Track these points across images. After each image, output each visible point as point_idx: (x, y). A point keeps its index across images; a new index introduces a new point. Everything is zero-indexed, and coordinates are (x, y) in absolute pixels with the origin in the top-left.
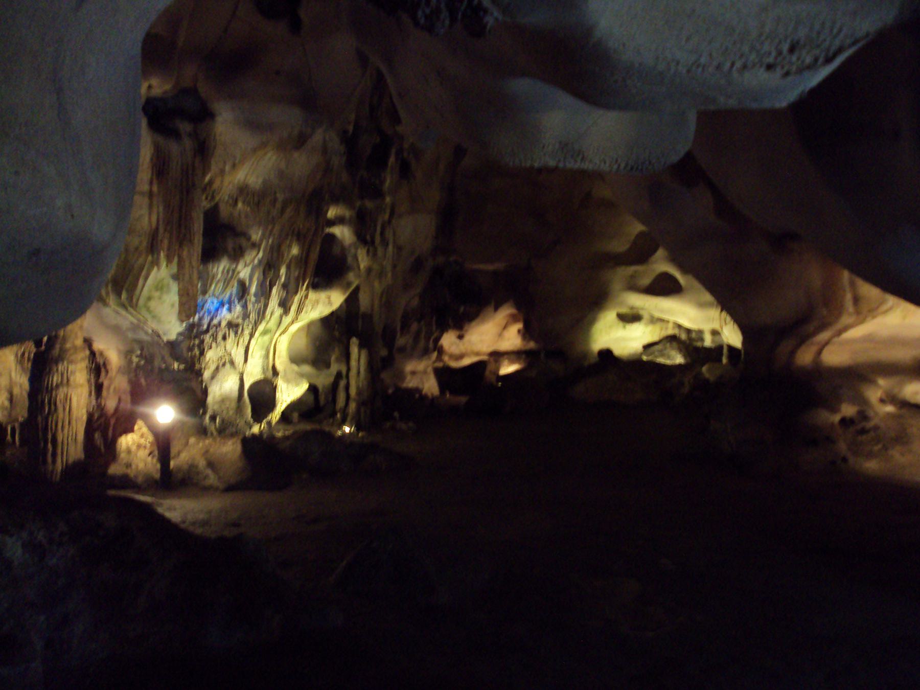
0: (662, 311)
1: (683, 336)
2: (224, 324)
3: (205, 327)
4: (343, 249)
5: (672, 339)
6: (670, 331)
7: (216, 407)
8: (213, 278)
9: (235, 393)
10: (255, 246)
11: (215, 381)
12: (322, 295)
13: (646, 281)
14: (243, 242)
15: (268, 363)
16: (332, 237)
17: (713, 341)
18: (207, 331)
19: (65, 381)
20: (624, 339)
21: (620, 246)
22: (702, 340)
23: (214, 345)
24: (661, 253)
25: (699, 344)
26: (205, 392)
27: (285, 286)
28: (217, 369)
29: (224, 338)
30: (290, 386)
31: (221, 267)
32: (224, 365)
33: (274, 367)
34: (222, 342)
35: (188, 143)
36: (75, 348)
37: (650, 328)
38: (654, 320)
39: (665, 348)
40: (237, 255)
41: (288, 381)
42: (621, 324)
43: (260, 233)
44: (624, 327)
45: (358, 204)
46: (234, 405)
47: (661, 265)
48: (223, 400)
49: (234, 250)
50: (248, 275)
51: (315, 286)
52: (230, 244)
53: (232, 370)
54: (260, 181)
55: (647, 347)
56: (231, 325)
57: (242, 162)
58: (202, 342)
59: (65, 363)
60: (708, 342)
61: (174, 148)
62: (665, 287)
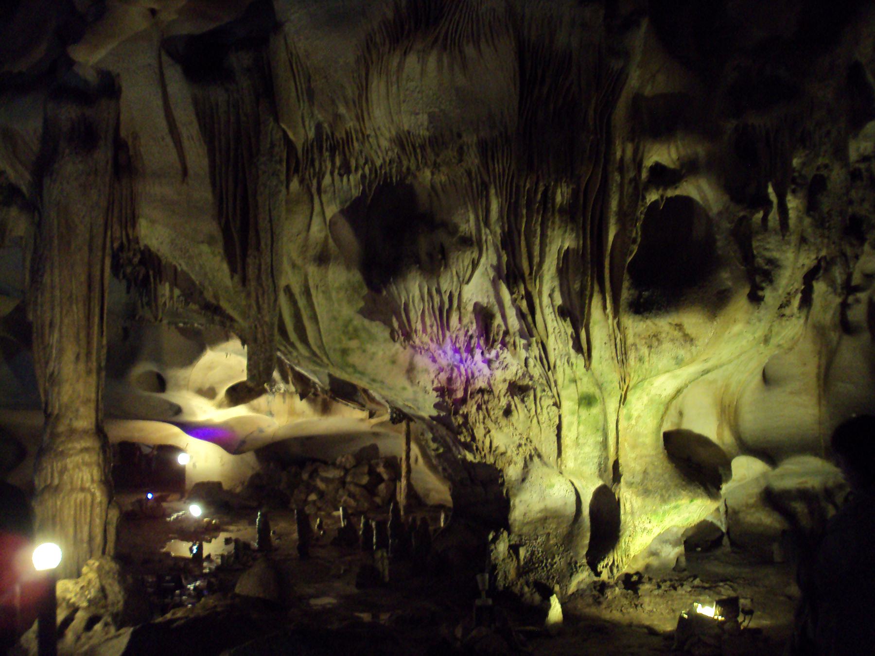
2: (501, 388)
3: (460, 394)
4: (709, 220)
7: (525, 530)
8: (406, 305)
9: (572, 509)
10: (467, 242)
11: (527, 484)
12: (663, 324)
14: (442, 236)
15: (607, 458)
16: (687, 201)
18: (464, 401)
19: (56, 482)
23: (491, 425)
26: (504, 505)
27: (563, 312)
28: (526, 466)
29: (508, 412)
30: (649, 501)
31: (413, 290)
32: (531, 457)
33: (616, 464)
34: (503, 422)
35: (245, 83)
36: (72, 432)
40: (434, 263)
41: (646, 492)
43: (472, 217)
45: (730, 125)
46: (563, 529)
48: (548, 517)
49: (431, 256)
50: (492, 300)
51: (641, 308)
52: (423, 245)
53: (545, 470)
54: (424, 118)
56: (518, 389)
57: (364, 89)
58: (466, 417)
59: (52, 456)
61: (219, 96)
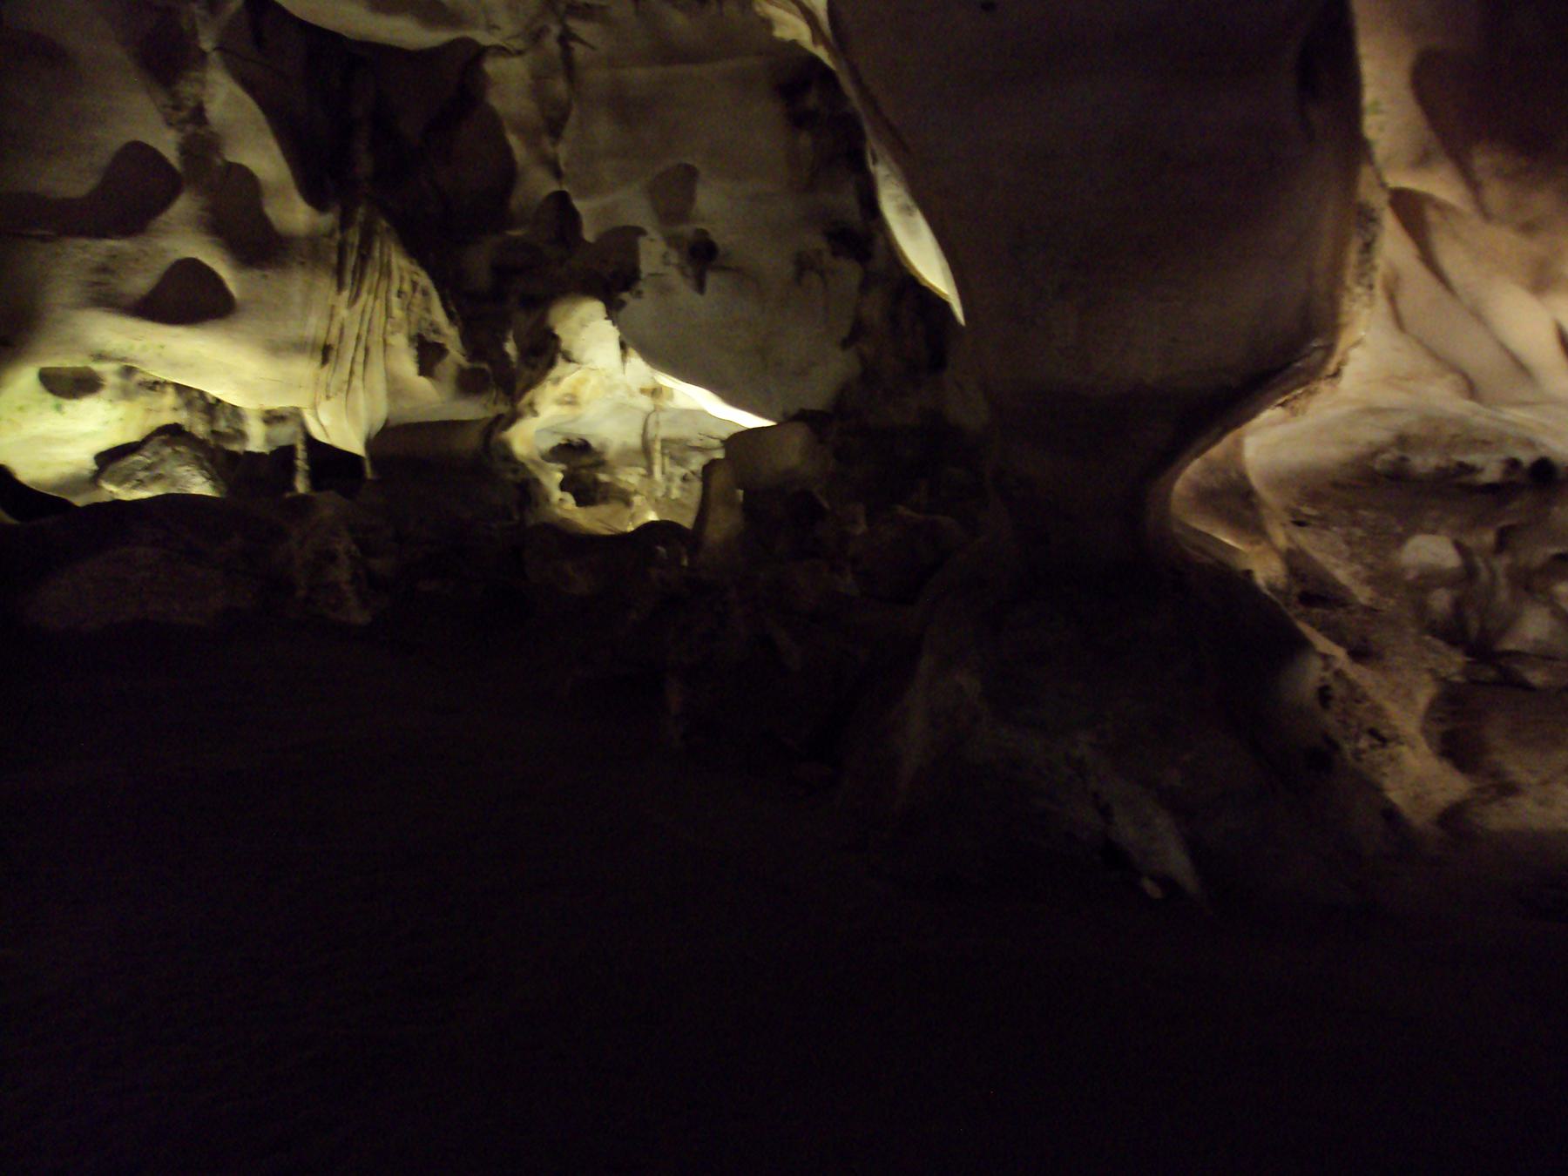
0: (174, 365)
1: (200, 429)
5: (172, 433)
6: (167, 411)
13: (141, 283)
17: (268, 440)
20: (47, 440)
21: (71, 179)
22: (241, 436)
24: (184, 206)
25: (235, 447)
37: (122, 409)
38: (137, 383)
39: (163, 460)
42: (51, 399)
44: (59, 408)
47: (182, 239)
55: (110, 459)
60: (257, 439)
62: (188, 300)
